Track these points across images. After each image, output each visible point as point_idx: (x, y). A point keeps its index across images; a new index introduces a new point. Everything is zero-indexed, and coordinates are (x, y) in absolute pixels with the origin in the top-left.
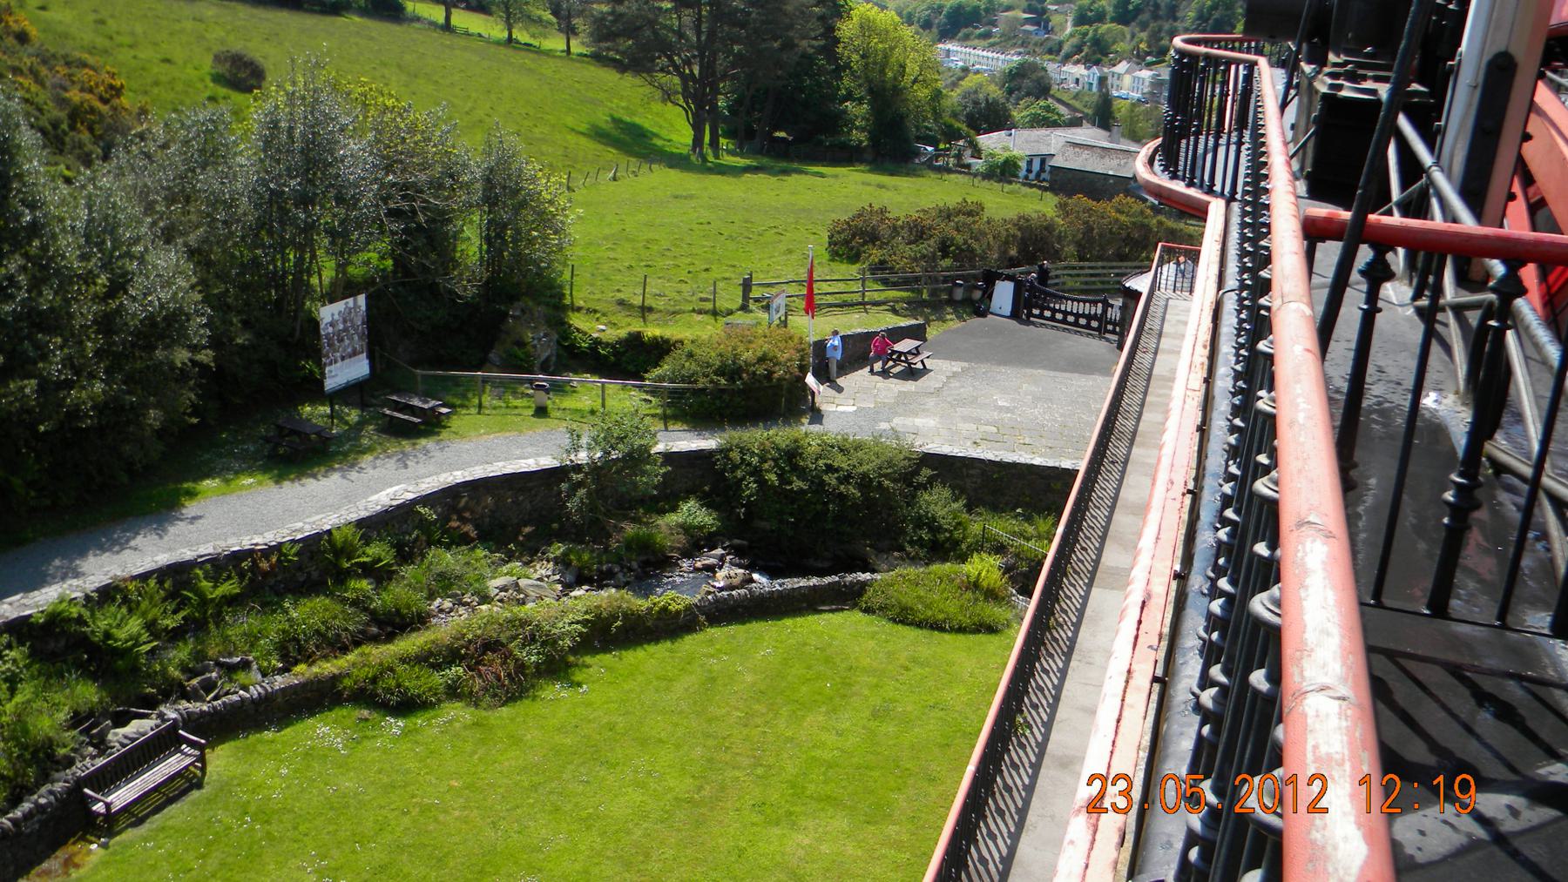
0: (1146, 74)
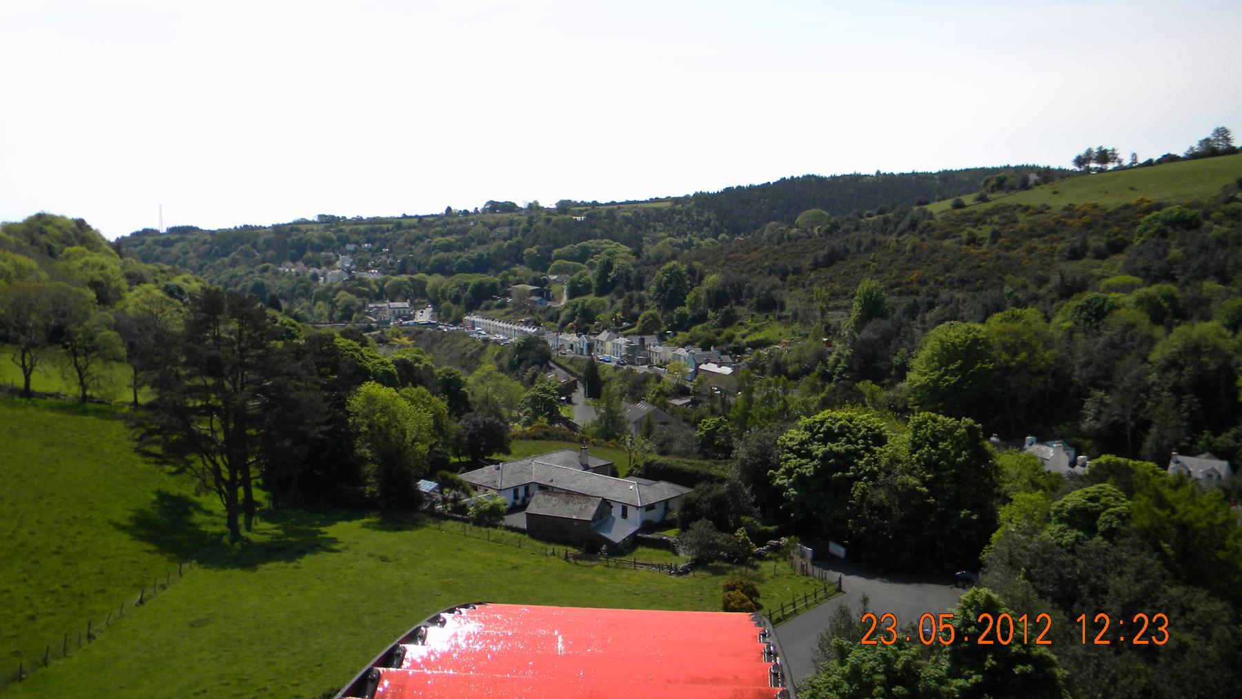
0: (622, 341)
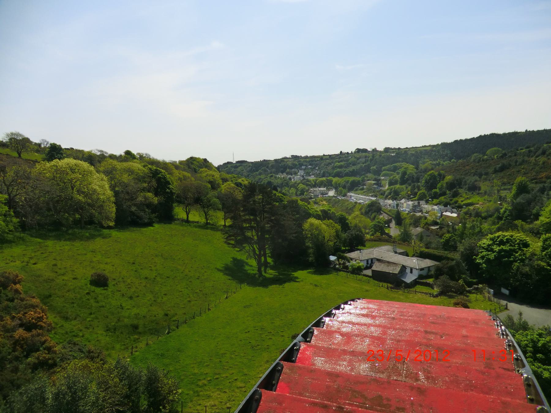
0: (410, 203)
